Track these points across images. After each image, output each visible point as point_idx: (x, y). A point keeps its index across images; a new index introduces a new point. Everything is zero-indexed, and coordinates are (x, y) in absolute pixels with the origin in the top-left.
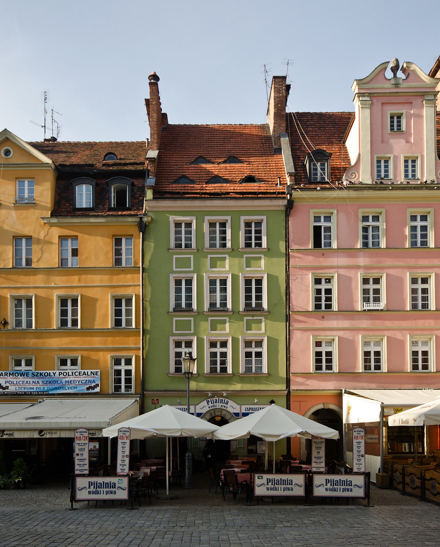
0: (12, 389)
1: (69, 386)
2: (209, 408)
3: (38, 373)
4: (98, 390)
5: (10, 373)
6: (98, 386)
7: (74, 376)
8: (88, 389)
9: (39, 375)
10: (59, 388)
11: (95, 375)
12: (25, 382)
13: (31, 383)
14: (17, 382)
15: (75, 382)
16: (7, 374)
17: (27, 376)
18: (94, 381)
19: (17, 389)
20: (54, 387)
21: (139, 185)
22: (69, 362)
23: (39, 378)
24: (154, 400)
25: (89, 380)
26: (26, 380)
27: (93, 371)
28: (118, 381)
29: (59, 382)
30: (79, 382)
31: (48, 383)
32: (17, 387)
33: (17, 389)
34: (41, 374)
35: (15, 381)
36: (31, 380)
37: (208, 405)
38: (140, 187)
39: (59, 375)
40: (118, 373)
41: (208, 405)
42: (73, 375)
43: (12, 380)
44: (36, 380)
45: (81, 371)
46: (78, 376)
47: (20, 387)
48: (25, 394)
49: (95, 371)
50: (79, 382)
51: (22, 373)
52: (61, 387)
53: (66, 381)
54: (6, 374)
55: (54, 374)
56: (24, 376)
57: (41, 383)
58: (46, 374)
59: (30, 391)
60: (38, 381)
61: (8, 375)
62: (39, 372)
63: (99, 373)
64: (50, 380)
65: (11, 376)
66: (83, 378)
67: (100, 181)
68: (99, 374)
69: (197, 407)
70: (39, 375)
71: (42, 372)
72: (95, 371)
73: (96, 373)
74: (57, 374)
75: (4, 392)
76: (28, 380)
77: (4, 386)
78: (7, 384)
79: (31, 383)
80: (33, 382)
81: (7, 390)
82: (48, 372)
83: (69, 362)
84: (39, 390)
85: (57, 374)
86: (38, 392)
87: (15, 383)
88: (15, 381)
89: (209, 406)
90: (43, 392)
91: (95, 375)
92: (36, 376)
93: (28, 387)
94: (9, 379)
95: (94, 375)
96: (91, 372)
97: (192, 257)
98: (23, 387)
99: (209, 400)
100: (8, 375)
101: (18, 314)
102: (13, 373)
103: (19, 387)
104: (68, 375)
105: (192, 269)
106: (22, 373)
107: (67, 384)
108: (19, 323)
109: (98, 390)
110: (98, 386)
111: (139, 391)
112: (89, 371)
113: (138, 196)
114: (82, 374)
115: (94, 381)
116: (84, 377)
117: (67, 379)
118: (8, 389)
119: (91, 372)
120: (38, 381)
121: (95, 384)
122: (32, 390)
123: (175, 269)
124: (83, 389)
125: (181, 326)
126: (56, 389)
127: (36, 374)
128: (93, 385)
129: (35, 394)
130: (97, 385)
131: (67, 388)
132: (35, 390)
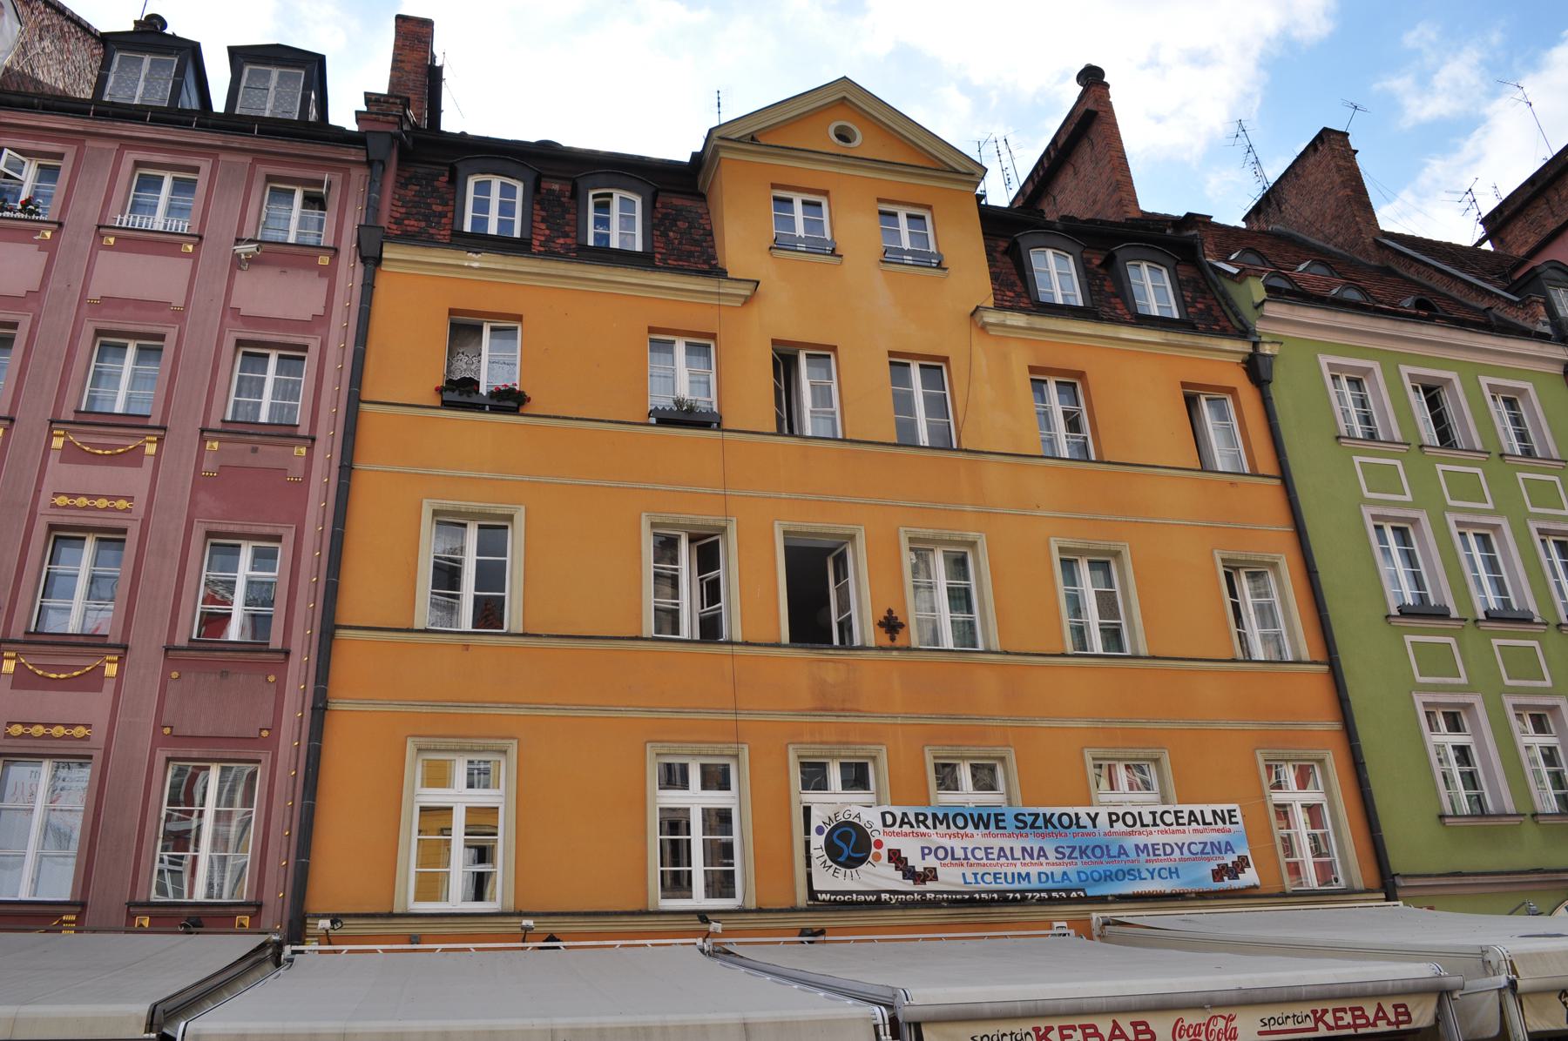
0: (951, 879)
1: (1150, 866)
3: (1037, 815)
4: (1249, 877)
5: (935, 816)
7: (1162, 827)
8: (1218, 874)
9: (1040, 822)
10: (1120, 875)
11: (1228, 825)
12: (996, 851)
13: (1018, 854)
14: (965, 849)
15: (1168, 850)
16: (926, 817)
17: (998, 827)
18: (1229, 847)
19: (970, 879)
20: (1101, 868)
23: (1043, 836)
26: (997, 843)
27: (1218, 808)
29: (1114, 851)
30: (1181, 849)
31: (1076, 854)
32: (969, 872)
33: (970, 879)
34: (1048, 821)
35: (957, 845)
36: (1018, 844)
39: (1112, 823)
42: (1155, 824)
43: (947, 842)
44: (1033, 843)
45: (1179, 808)
46: (1175, 827)
47: (981, 871)
48: (1003, 900)
49: (1226, 807)
50: (1181, 849)
51: (980, 816)
52: (1126, 867)
53: (1137, 846)
54: (921, 819)
55: (1094, 820)
56: (987, 827)
57: (1052, 855)
58: (1065, 820)
59: (1016, 886)
60: (1041, 849)
61: (930, 822)
62: (1041, 810)
64: (1077, 842)
65: (942, 829)
66: (1190, 835)
70: (1040, 822)
71: (1048, 811)
72: (1226, 807)
74: (1103, 820)
75: (923, 893)
76: (1007, 843)
77: (919, 869)
78: (931, 861)
79: (1018, 854)
80: (1024, 849)
81: (930, 886)
82: (1071, 811)
84: (1050, 885)
85: (1103, 820)
86: (1048, 891)
87: (959, 853)
88: (957, 845)
90: (1068, 891)
92: (1032, 826)
93: (1009, 870)
94: (938, 837)
98: (992, 870)
100: (930, 822)
102: (946, 816)
103: (975, 869)
104: (1143, 825)
106: (980, 816)
107: (1144, 856)
109: (1249, 877)
110: (1248, 865)
112: (1208, 809)
114: (1186, 820)
115: (1229, 847)
116: (1195, 831)
117: (1141, 840)
118: (935, 878)
120: (1041, 849)
122: (1024, 885)
124: (1200, 876)
126: (1109, 877)
127: (1029, 820)
128: (1229, 859)
129: (1041, 900)
130: (1241, 864)
131: (1145, 874)
132: (1035, 884)
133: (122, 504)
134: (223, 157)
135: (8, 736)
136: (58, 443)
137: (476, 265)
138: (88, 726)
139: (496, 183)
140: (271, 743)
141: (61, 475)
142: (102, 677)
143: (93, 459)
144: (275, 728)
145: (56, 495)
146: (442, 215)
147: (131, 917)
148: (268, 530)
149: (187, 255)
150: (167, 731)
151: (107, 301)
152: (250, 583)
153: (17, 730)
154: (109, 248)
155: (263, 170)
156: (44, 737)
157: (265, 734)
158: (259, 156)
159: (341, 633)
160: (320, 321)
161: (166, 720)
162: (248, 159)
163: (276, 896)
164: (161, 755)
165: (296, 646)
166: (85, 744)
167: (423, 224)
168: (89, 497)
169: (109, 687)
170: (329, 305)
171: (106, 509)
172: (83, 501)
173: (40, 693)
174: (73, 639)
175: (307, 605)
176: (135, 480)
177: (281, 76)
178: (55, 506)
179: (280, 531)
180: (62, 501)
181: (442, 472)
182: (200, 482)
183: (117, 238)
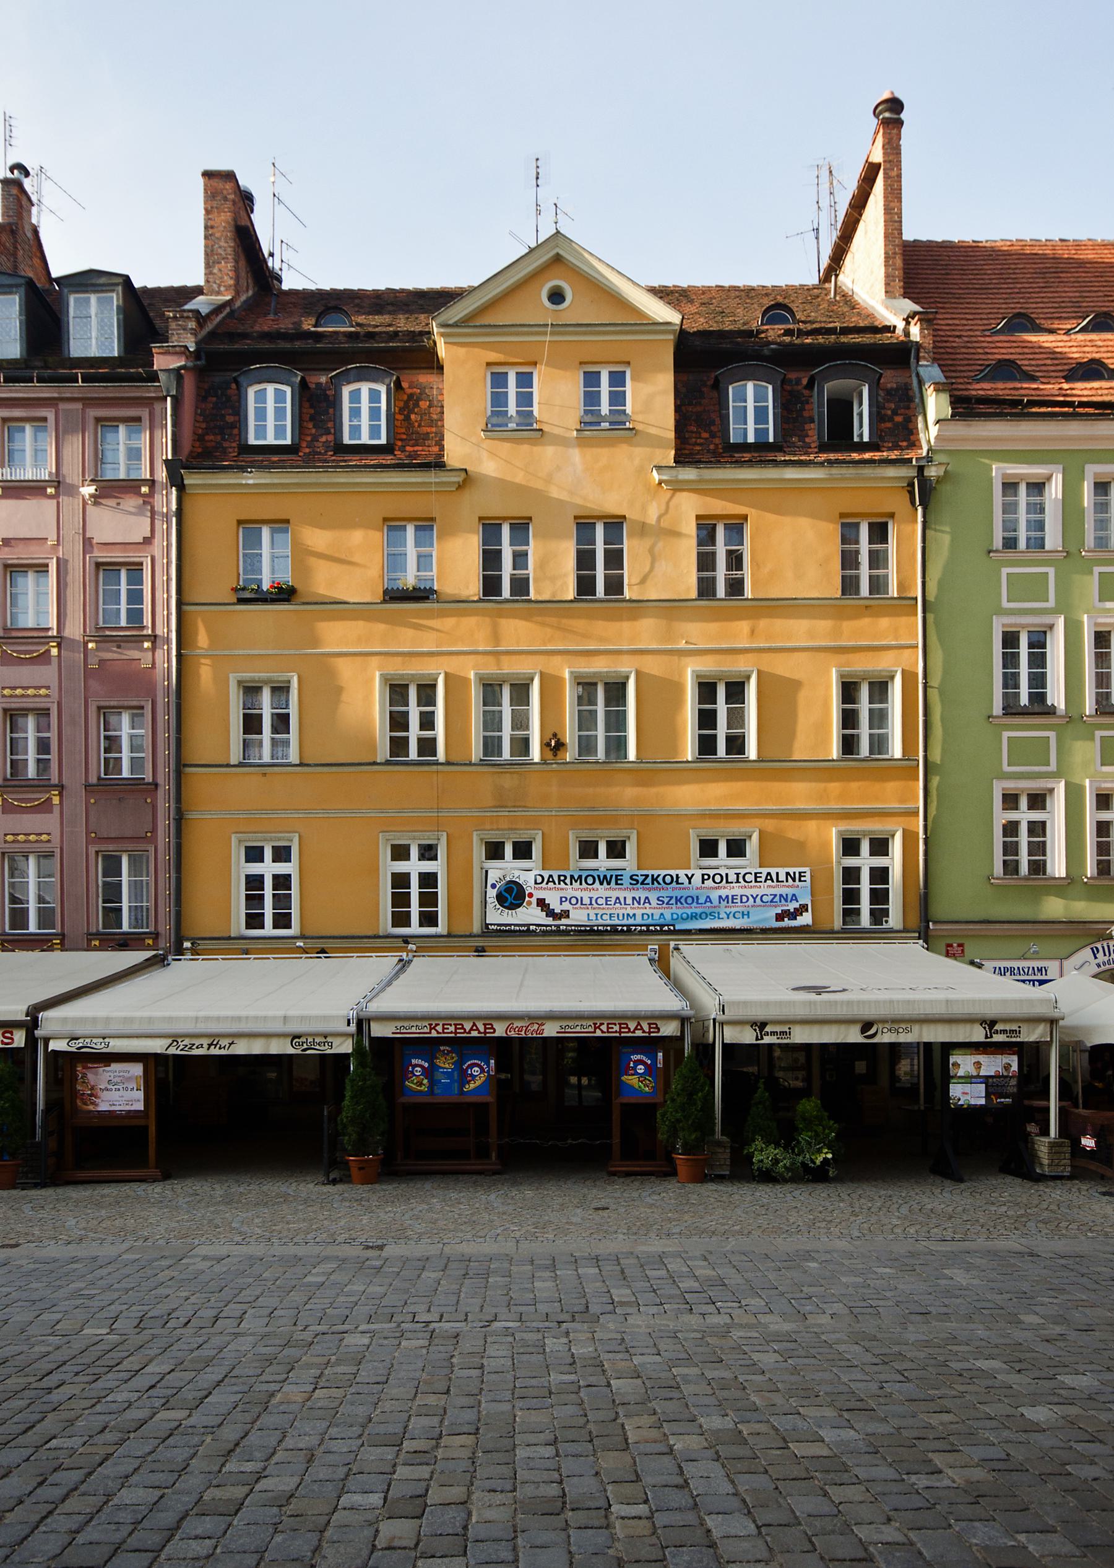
0: (578, 917)
1: (728, 910)
2: (1099, 966)
3: (647, 876)
4: (806, 919)
5: (572, 877)
6: (807, 910)
7: (743, 883)
8: (779, 917)
9: (649, 880)
10: (704, 916)
11: (797, 882)
12: (613, 900)
13: (629, 901)
14: (591, 898)
15: (744, 899)
16: (566, 877)
17: (617, 884)
19: (593, 917)
20: (689, 911)
21: (889, 386)
22: (722, 848)
23: (649, 890)
24: (951, 945)
25: (781, 896)
26: (614, 894)
27: (791, 870)
28: (850, 896)
29: (702, 900)
30: (755, 899)
31: (673, 901)
32: (592, 913)
33: (593, 917)
34: (654, 879)
35: (586, 896)
36: (629, 895)
37: (1096, 958)
38: (892, 389)
39: (703, 880)
40: (851, 875)
41: (1096, 958)
42: (738, 882)
43: (578, 894)
44: (641, 894)
45: (759, 870)
46: (753, 884)
47: (600, 912)
48: (614, 930)
49: (797, 870)
50: (755, 899)
51: (605, 877)
52: (708, 911)
53: (720, 897)
54: (562, 879)
55: (690, 879)
56: (609, 883)
57: (654, 902)
58: (668, 879)
59: (625, 922)
60: (647, 898)
61: (568, 881)
62: (650, 872)
63: (808, 875)
64: (678, 893)
65: (576, 885)
66: (766, 889)
67: (792, 376)
68: (808, 878)
69: (1065, 963)
70: (649, 880)
71: (656, 873)
73: (800, 876)
74: (697, 880)
75: (558, 926)
76: (621, 895)
77: (557, 911)
78: (566, 906)
79: (629, 901)
80: (634, 898)
81: (564, 921)
82: (673, 873)
83: (722, 848)
84: (650, 921)
85: (697, 880)
86: (648, 926)
87: (586, 901)
88: (586, 896)
89: (1097, 961)
90: (662, 926)
91: (797, 882)
92: (642, 883)
93: (621, 912)
94: (573, 890)
95: (794, 880)
96: (788, 874)
97: (1051, 571)
98: (609, 912)
99: (1099, 946)
100: (568, 881)
101: (586, 720)
102: (580, 877)
103: (596, 911)
104: (727, 882)
105: (1051, 603)
106: (605, 877)
107: (724, 904)
108: (586, 746)
109: (806, 919)
110: (807, 910)
111: (914, 921)
113: (889, 412)
114: (763, 879)
115: (794, 898)
116: (769, 886)
117: (723, 893)
118: (568, 916)
119: (788, 874)
120: (647, 898)
121: (797, 905)
122: (631, 921)
123: (1005, 604)
124: (767, 917)
125: (1021, 752)
126: (694, 917)
127: (641, 879)
128: (792, 906)
129: (641, 931)
130: (803, 908)
131: (723, 915)
132: (639, 921)
133: (43, 692)
134: (62, 406)
135: (6, 842)
137: (251, 482)
138: (49, 834)
139: (270, 388)
140: (153, 840)
142: (52, 805)
144: (154, 830)
146: (233, 426)
147: (89, 941)
148: (135, 703)
149: (51, 497)
150: (93, 835)
153: (9, 838)
155: (93, 413)
156: (25, 841)
158: (88, 402)
160: (148, 541)
161: (91, 828)
162: (79, 406)
163: (166, 927)
164: (92, 850)
165: (160, 780)
166: (49, 845)
167: (219, 438)
168: (23, 688)
169: (56, 810)
170: (153, 531)
172: (18, 692)
174: (32, 783)
176: (47, 674)
179: (142, 703)
181: (241, 652)
182: (88, 673)
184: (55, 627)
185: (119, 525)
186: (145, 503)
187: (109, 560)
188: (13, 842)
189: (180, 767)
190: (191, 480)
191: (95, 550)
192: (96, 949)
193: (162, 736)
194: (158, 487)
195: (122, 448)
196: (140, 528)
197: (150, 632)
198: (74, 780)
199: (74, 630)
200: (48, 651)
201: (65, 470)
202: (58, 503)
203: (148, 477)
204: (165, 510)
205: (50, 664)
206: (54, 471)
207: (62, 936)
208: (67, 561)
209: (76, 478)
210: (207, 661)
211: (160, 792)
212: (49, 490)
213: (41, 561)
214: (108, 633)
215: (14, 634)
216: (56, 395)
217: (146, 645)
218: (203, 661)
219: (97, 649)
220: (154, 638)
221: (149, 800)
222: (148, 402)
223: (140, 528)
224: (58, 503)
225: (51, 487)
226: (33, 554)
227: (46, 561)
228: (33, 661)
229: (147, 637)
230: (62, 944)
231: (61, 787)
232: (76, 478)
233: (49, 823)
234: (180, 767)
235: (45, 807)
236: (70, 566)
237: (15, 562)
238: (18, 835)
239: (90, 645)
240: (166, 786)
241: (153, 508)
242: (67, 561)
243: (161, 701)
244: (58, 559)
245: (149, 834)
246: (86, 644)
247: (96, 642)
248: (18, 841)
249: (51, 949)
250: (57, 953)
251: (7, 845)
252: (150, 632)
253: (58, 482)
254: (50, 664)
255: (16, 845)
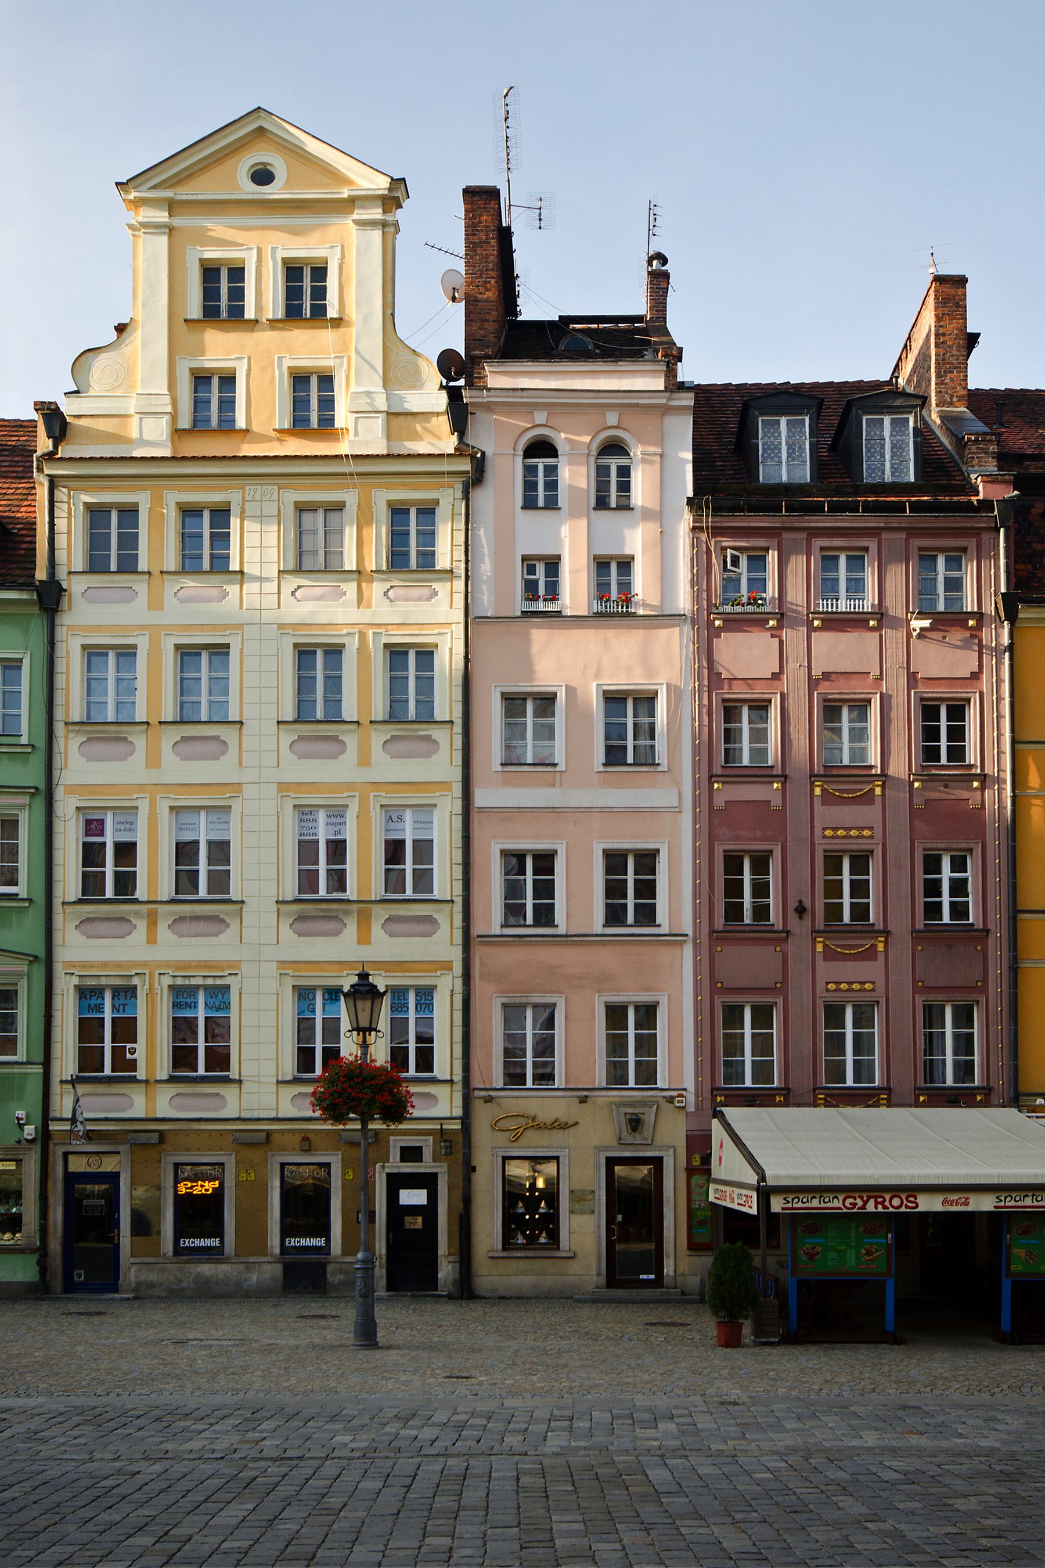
135: (827, 990)
136: (818, 791)
138: (873, 983)
140: (984, 990)
141: (826, 815)
142: (876, 951)
143: (842, 801)
144: (985, 979)
145: (825, 829)
147: (917, 1097)
148: (963, 846)
149: (873, 629)
151: (826, 676)
152: (951, 880)
154: (816, 629)
155: (917, 543)
157: (980, 984)
158: (913, 532)
159: (1021, 916)
160: (976, 676)
162: (903, 535)
163: (1000, 1083)
164: (919, 1000)
170: (981, 666)
171: (858, 837)
173: (840, 963)
175: (998, 898)
176: (870, 814)
177: (893, 421)
178: (825, 837)
179: (972, 846)
180: (828, 833)
182: (913, 813)
183: (823, 620)
184: (879, 765)
185: (944, 660)
186: (972, 636)
187: (935, 695)
188: (848, 990)
189: (1015, 912)
190: (1025, 613)
191: (920, 685)
192: (923, 1105)
193: (993, 880)
194: (985, 620)
195: (941, 579)
196: (965, 663)
197: (979, 771)
198: (901, 926)
199: (898, 768)
200: (872, 790)
201: (888, 602)
202: (881, 636)
203: (976, 610)
204: (994, 645)
205: (873, 804)
206: (876, 602)
207: (888, 1090)
208: (891, 696)
209: (899, 611)
210: (1038, 802)
211: (991, 940)
212: (872, 623)
213: (863, 696)
214: (934, 772)
215: (835, 772)
216: (882, 525)
217: (975, 784)
218: (1034, 801)
219: (922, 789)
220: (983, 778)
221: (979, 948)
222: (975, 533)
223: (965, 663)
224: (881, 636)
225: (873, 619)
226: (857, 689)
227: (870, 696)
228: (855, 801)
229: (975, 777)
230: (889, 1100)
231: (886, 933)
232: (899, 611)
233: (870, 971)
234: (1015, 912)
235: (870, 954)
236: (894, 701)
237: (837, 696)
238: (853, 983)
239: (916, 785)
240: (999, 934)
241: (980, 641)
242: (891, 696)
243: (992, 843)
244: (882, 694)
245: (980, 984)
246: (911, 784)
247: (922, 781)
248: (852, 990)
249: (876, 1105)
250: (883, 1110)
251: (829, 994)
252: (979, 771)
253: (880, 614)
254: (873, 804)
255: (852, 994)
